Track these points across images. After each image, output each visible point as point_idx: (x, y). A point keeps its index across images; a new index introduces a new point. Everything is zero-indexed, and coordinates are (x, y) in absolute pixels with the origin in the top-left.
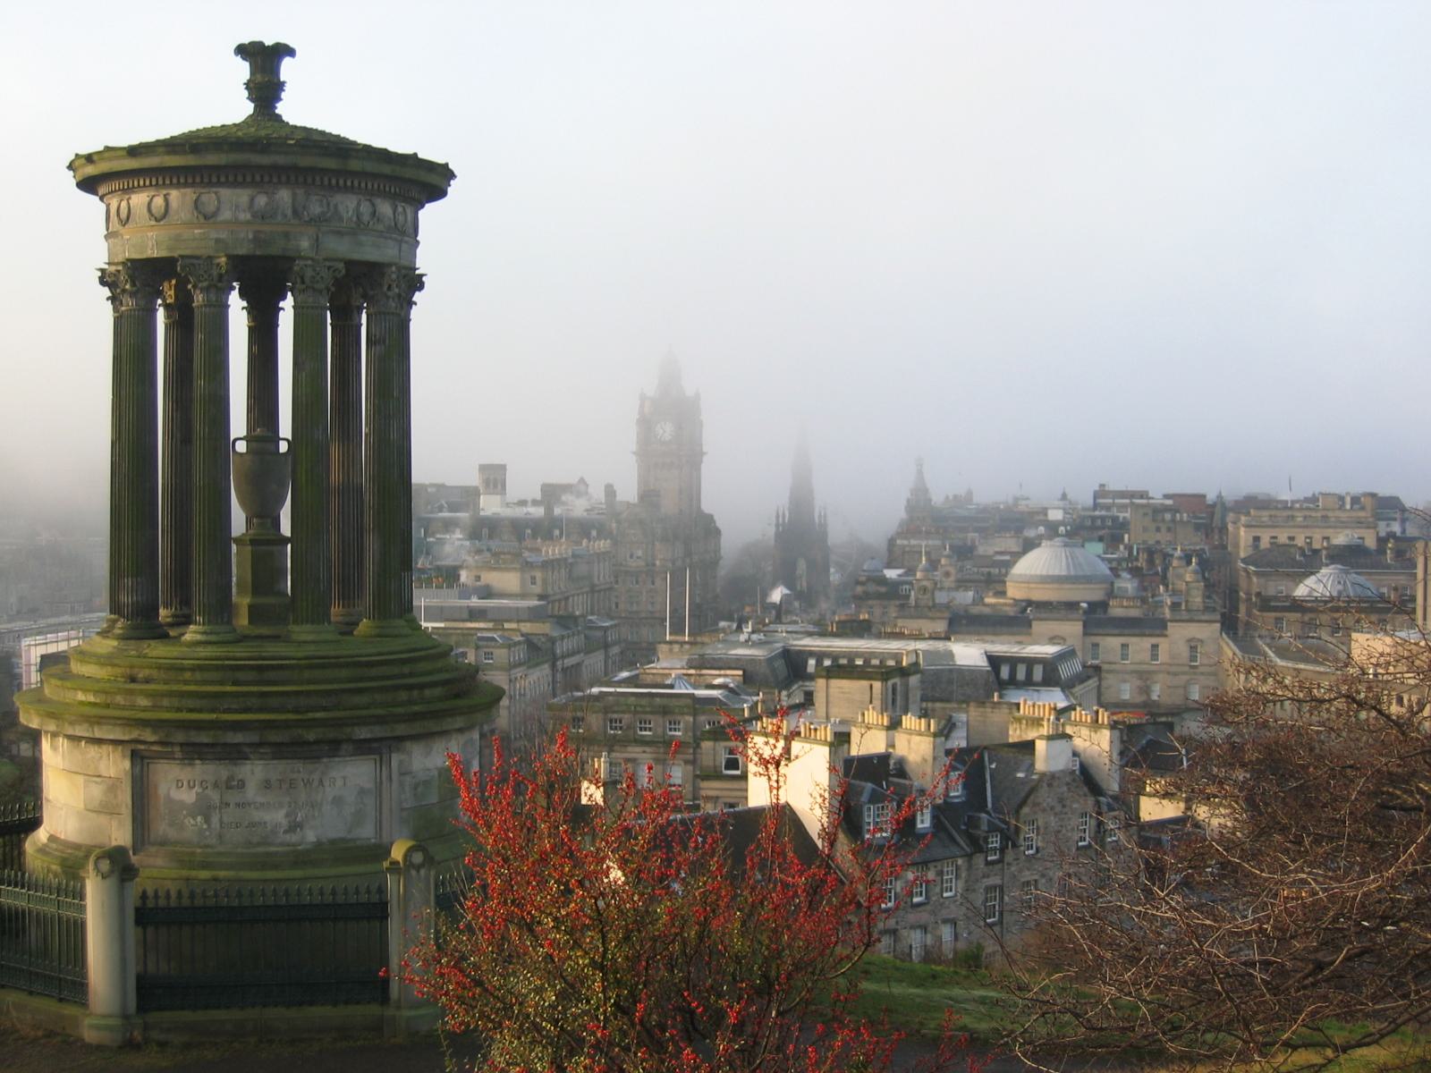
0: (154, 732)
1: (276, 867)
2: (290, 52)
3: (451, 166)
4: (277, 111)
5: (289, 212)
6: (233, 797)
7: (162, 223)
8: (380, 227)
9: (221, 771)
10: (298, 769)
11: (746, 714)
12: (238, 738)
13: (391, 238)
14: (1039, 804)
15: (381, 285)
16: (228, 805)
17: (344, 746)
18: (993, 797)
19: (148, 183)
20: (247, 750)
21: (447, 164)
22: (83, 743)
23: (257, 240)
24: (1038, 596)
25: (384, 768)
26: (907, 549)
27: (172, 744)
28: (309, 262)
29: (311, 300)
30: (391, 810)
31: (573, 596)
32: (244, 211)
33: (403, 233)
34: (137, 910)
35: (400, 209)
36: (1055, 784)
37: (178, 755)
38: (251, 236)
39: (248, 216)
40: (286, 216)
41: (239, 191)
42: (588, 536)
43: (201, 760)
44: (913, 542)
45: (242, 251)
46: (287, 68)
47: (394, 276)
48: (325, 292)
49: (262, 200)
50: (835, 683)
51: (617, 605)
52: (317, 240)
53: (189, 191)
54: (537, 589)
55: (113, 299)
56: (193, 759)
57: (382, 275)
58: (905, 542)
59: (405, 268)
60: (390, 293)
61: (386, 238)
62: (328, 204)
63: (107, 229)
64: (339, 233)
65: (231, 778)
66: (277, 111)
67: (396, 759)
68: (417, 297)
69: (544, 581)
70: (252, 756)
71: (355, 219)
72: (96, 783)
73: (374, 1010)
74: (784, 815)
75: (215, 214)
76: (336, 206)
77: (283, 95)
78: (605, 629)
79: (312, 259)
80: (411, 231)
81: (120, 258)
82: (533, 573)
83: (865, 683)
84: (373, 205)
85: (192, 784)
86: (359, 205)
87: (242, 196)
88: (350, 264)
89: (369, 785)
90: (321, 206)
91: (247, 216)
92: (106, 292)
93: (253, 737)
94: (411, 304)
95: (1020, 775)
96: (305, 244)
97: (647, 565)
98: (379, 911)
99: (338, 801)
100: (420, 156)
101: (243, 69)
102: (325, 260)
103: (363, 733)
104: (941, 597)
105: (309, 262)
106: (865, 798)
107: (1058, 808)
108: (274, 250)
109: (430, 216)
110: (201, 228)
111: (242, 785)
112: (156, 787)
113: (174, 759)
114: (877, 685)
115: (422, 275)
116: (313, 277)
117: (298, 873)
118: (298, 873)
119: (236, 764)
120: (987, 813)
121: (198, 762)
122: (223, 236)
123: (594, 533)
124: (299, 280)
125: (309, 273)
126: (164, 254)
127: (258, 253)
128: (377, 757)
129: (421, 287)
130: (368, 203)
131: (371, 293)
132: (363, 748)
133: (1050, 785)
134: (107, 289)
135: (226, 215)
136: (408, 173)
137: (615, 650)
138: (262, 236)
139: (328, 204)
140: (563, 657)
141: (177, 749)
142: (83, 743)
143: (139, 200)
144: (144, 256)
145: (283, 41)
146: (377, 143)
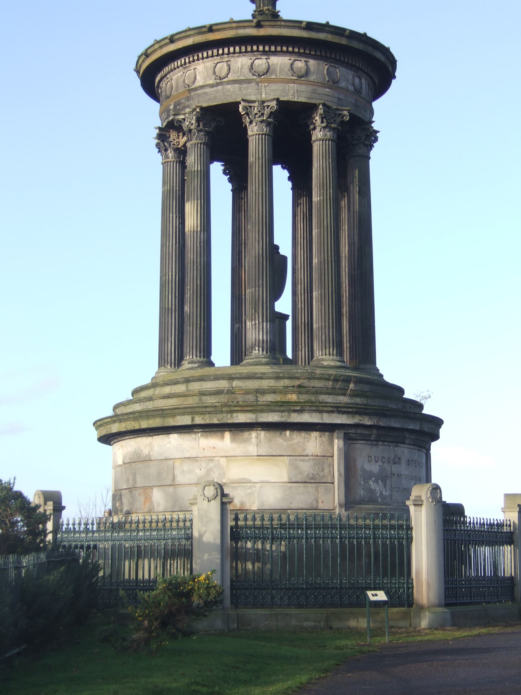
6: (395, 469)
7: (303, 79)
16: (394, 475)
37: (373, 437)
43: (383, 441)
49: (357, 80)
65: (395, 456)
72: (303, 460)
85: (377, 459)
91: (351, 88)
112: (355, 461)
113: (370, 440)
119: (397, 446)
121: (380, 443)
143: (276, 60)
144: (286, 99)
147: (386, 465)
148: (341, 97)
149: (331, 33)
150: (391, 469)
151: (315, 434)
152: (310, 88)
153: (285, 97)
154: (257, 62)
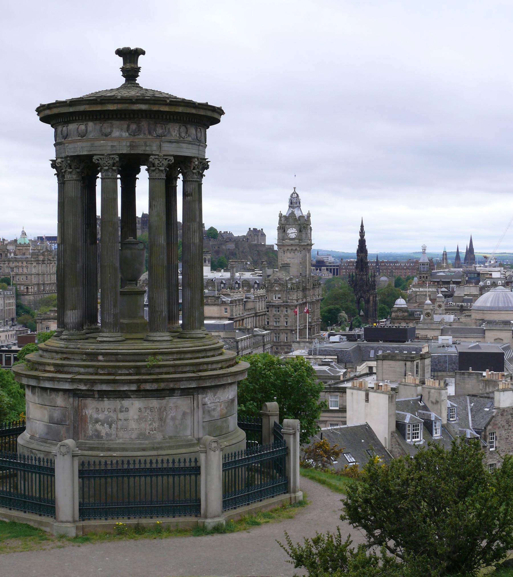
0: (85, 385)
1: (144, 450)
2: (143, 53)
3: (222, 109)
4: (137, 82)
5: (147, 132)
6: (121, 416)
7: (84, 138)
8: (190, 139)
9: (117, 403)
10: (154, 403)
11: (342, 378)
12: (125, 388)
13: (195, 144)
14: (496, 424)
15: (190, 167)
16: (121, 420)
17: (176, 392)
18: (472, 420)
19: (77, 118)
20: (129, 393)
21: (221, 107)
22: (49, 391)
23: (131, 146)
24: (488, 317)
25: (195, 402)
26: (418, 293)
27: (94, 391)
28: (157, 157)
29: (157, 175)
30: (198, 422)
31: (246, 318)
32: (125, 132)
33: (200, 141)
34: (79, 471)
35: (199, 130)
36: (505, 414)
37: (96, 396)
38: (128, 144)
39: (127, 134)
40: (145, 134)
41: (122, 122)
42: (253, 287)
43: (107, 398)
44: (421, 289)
45: (124, 152)
46: (141, 60)
47: (197, 163)
48: (164, 172)
49: (133, 127)
50: (386, 362)
51: (268, 322)
52: (160, 146)
53: (98, 122)
54: (228, 315)
55: (57, 175)
56: (104, 398)
57: (191, 162)
58: (417, 290)
59: (201, 159)
60: (194, 171)
61: (192, 144)
62: (165, 128)
63: (56, 141)
64: (170, 142)
65: (122, 407)
66: (137, 82)
67: (200, 396)
68: (205, 172)
69: (232, 311)
70: (132, 397)
71: (178, 135)
73: (192, 519)
74: (366, 431)
75: (110, 133)
76: (169, 129)
77: (139, 74)
78: (263, 336)
79: (158, 155)
80: (203, 140)
81: (63, 155)
82: (226, 307)
83: (403, 363)
84: (187, 128)
86: (180, 128)
87: (124, 124)
88: (175, 157)
89: (188, 411)
90: (162, 129)
91: (125, 134)
92: (55, 171)
93: (134, 387)
94: (202, 176)
95: (487, 409)
96: (155, 148)
97: (284, 302)
98: (196, 471)
99: (173, 419)
100: (209, 104)
101: (120, 61)
102: (164, 155)
103: (184, 385)
104: (437, 318)
105: (157, 157)
106: (407, 421)
107: (507, 427)
108: (140, 151)
109: (212, 131)
110: (104, 140)
111: (127, 410)
113: (94, 398)
114: (409, 363)
115: (208, 162)
116: (158, 164)
117: (155, 453)
118: (155, 453)
120: (470, 429)
121: (105, 399)
122: (115, 144)
123: (256, 286)
124: (152, 165)
125: (157, 162)
126: (85, 153)
127: (132, 152)
128: (192, 396)
129: (207, 168)
130: (184, 127)
131: (185, 171)
132: (186, 392)
133: (502, 415)
134: (55, 169)
135: (116, 133)
136: (202, 112)
137: (268, 346)
138: (134, 144)
139: (165, 128)
140: (243, 350)
141: (96, 393)
142: (49, 391)
143: (72, 127)
145: (139, 47)
146: (188, 98)
147: (111, 414)
148: (114, 144)
149: (88, 104)
150: (117, 416)
151: (61, 393)
152: (89, 144)
153: (75, 152)
154: (65, 129)
